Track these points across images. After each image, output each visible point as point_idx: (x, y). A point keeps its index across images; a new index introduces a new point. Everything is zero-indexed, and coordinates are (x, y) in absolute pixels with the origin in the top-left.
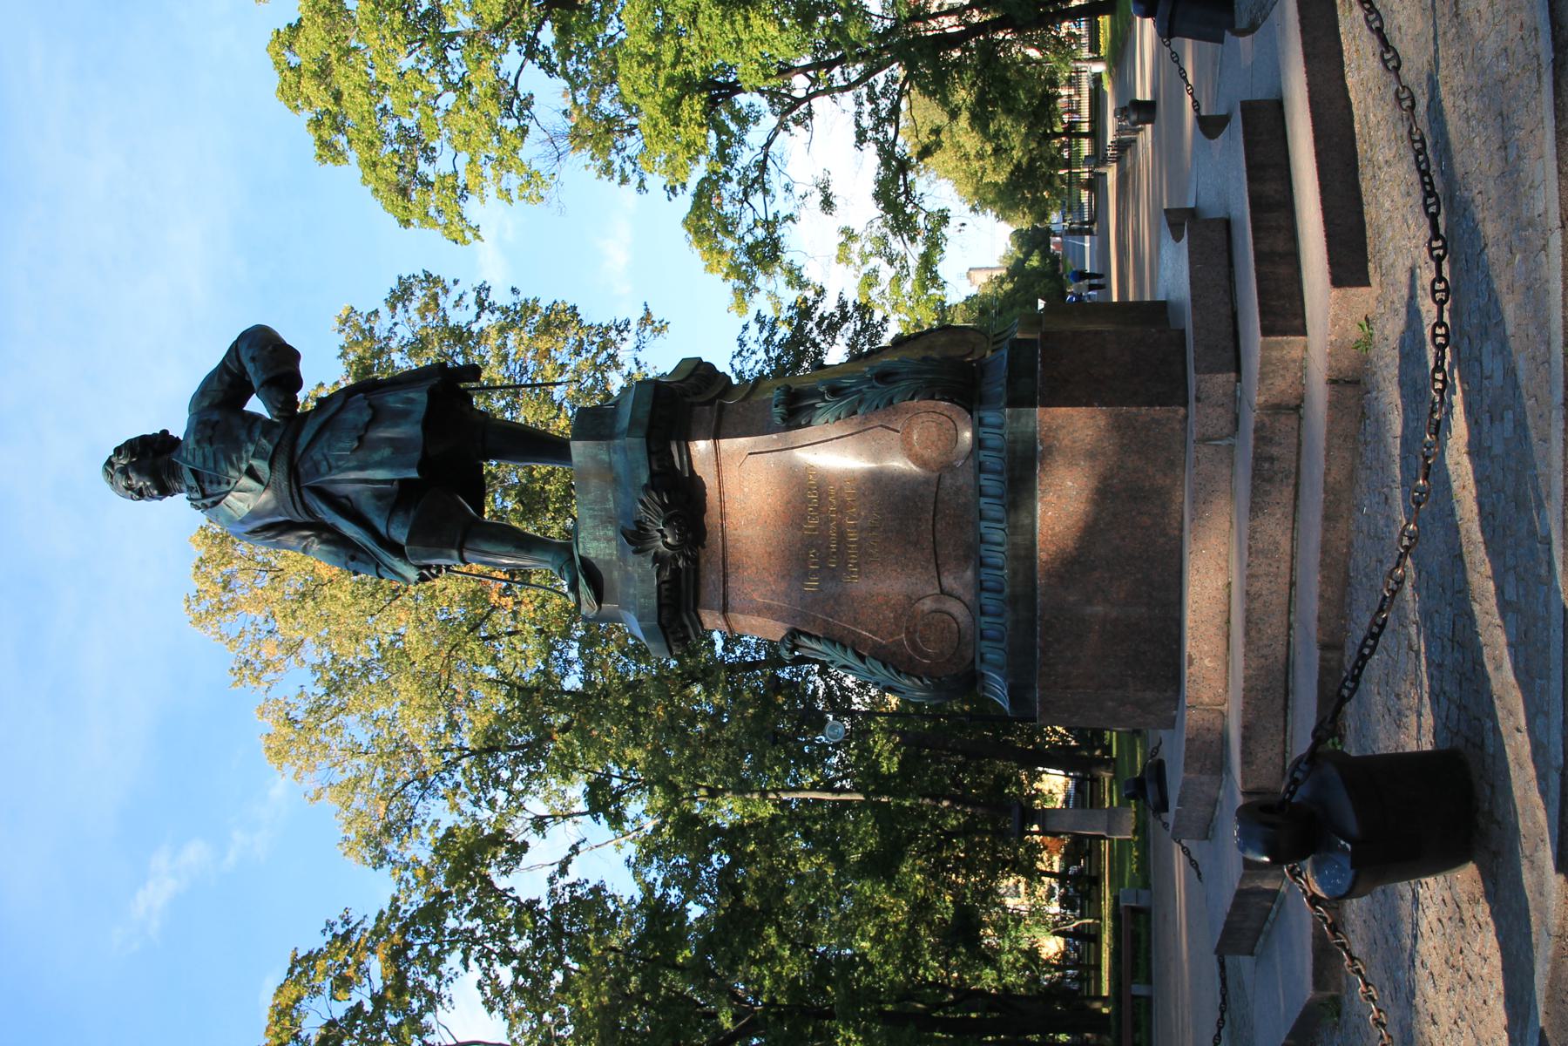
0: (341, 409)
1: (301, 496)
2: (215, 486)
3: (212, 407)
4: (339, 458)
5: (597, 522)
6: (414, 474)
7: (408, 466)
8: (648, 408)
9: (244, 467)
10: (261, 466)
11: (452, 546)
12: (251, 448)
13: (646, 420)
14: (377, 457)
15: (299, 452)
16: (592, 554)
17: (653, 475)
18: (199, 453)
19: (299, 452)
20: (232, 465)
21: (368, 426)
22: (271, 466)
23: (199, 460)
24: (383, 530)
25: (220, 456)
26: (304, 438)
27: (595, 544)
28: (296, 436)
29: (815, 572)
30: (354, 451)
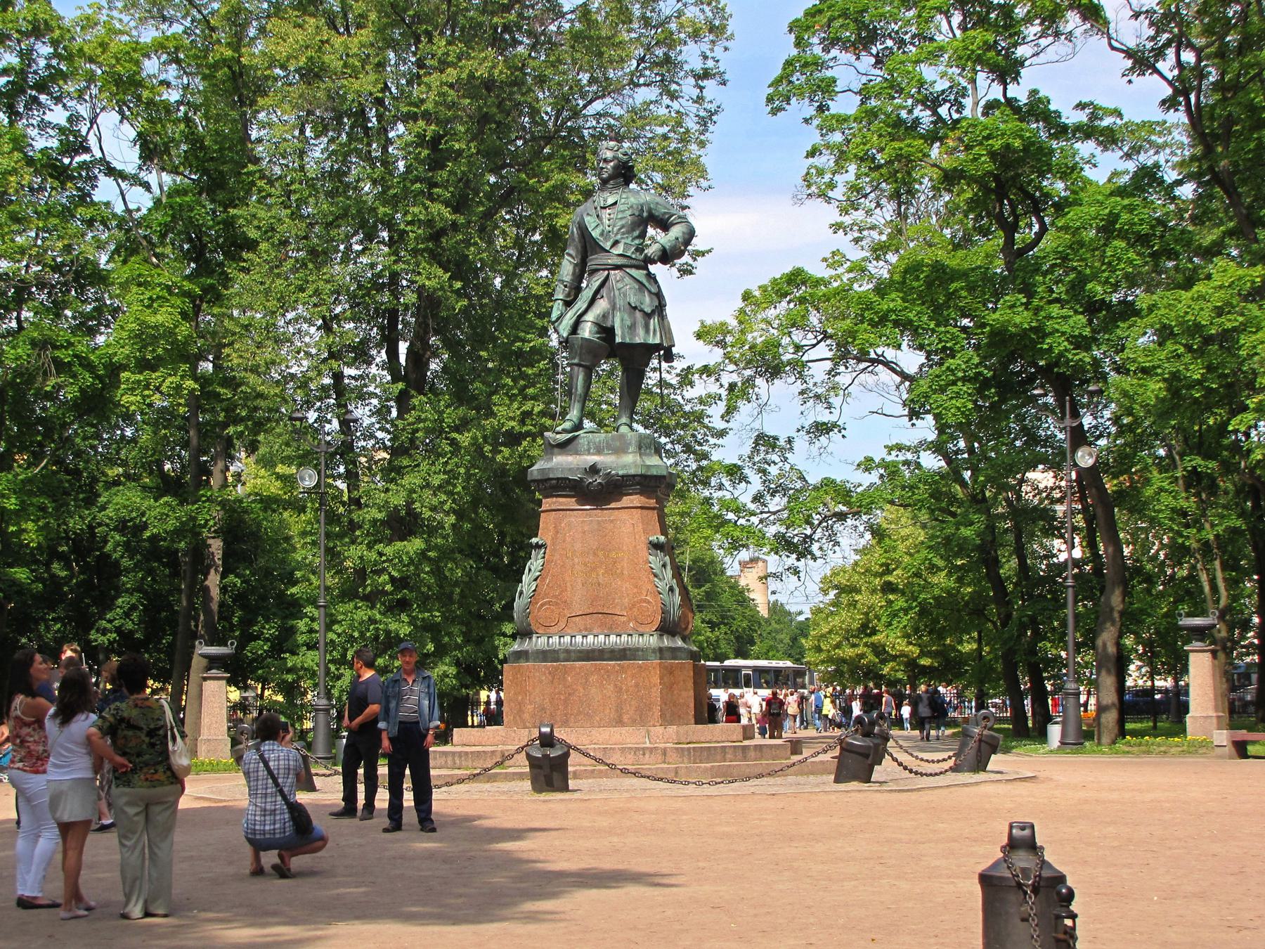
0: (650, 292)
3: (650, 211)
4: (625, 295)
6: (618, 340)
7: (623, 337)
9: (619, 237)
10: (619, 249)
11: (581, 359)
12: (629, 241)
14: (626, 317)
17: (623, 476)
18: (625, 207)
21: (642, 310)
23: (622, 208)
25: (623, 222)
26: (633, 272)
28: (637, 267)
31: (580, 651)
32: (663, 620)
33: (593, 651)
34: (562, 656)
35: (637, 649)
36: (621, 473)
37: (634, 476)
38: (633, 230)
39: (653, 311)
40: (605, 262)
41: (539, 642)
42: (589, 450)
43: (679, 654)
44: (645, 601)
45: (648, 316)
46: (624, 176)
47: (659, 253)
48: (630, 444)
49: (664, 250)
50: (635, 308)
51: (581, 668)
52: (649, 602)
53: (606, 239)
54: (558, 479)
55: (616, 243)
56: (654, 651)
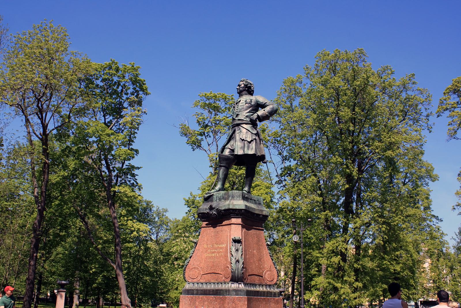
8: (238, 208)
13: (234, 208)
15: (243, 125)
16: (214, 197)
22: (239, 120)
24: (226, 147)
30: (241, 139)
31: (202, 290)
32: (232, 276)
34: (195, 292)
35: (221, 290)
36: (223, 208)
38: (246, 110)
39: (252, 141)
42: (216, 200)
43: (240, 293)
45: (250, 142)
46: (247, 91)
48: (230, 196)
49: (258, 116)
50: (243, 140)
51: (202, 298)
55: (237, 115)
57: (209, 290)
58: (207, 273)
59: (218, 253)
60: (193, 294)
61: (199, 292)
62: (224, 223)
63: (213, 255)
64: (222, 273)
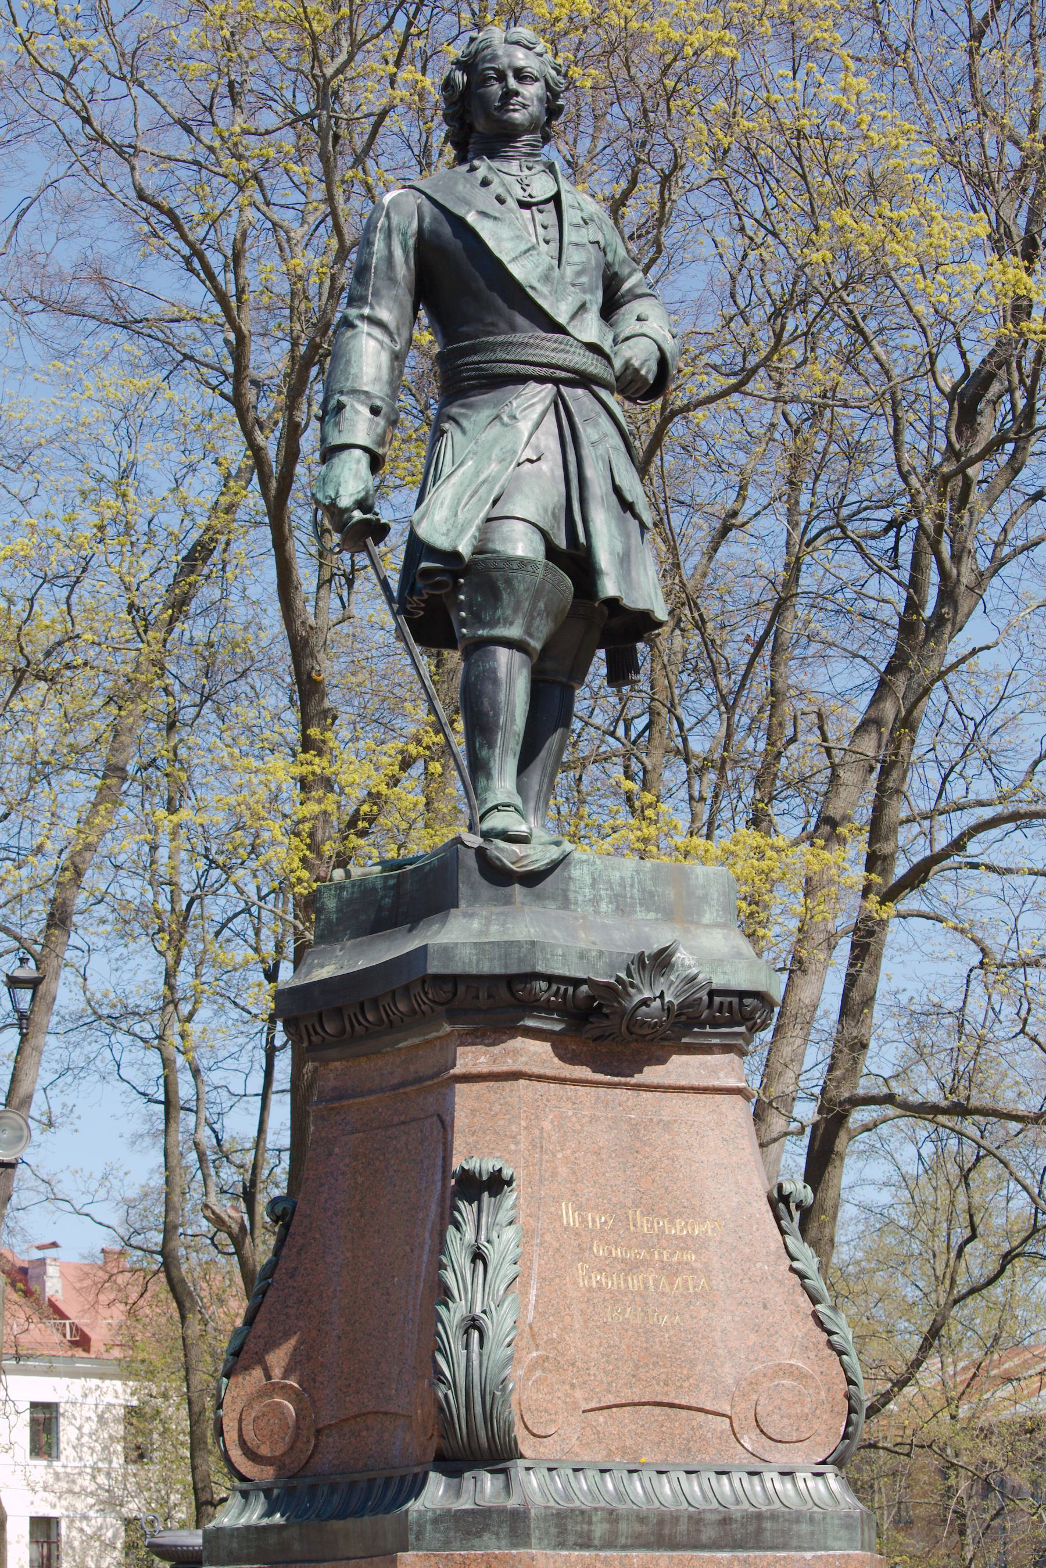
1: (542, 380)
2: (540, 230)
5: (617, 889)
15: (604, 394)
16: (575, 873)
19: (604, 394)
20: (579, 274)
27: (588, 880)
29: (584, 1221)
30: (617, 490)
31: (642, 1519)
33: (675, 1518)
34: (599, 1530)
35: (797, 1518)
37: (742, 994)
40: (558, 358)
41: (533, 1487)
42: (595, 901)
44: (791, 1372)
47: (654, 367)
48: (705, 899)
52: (801, 1376)
53: (558, 295)
54: (550, 979)
56: (848, 1523)
57: (697, 1520)
58: (611, 1400)
59: (671, 1271)
60: (585, 1543)
61: (623, 1526)
62: (651, 1074)
63: (635, 1283)
64: (727, 1409)
